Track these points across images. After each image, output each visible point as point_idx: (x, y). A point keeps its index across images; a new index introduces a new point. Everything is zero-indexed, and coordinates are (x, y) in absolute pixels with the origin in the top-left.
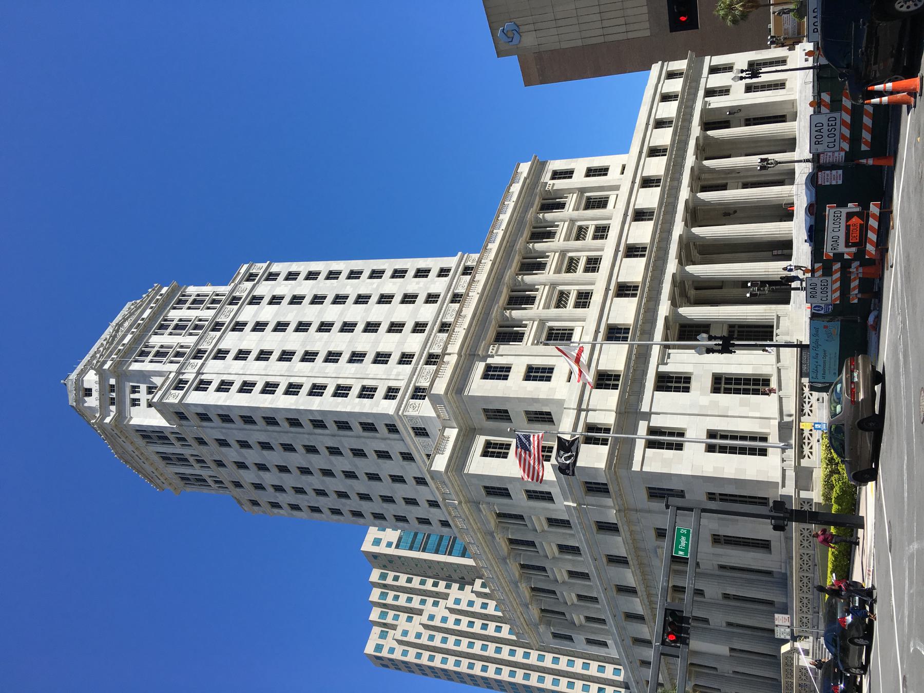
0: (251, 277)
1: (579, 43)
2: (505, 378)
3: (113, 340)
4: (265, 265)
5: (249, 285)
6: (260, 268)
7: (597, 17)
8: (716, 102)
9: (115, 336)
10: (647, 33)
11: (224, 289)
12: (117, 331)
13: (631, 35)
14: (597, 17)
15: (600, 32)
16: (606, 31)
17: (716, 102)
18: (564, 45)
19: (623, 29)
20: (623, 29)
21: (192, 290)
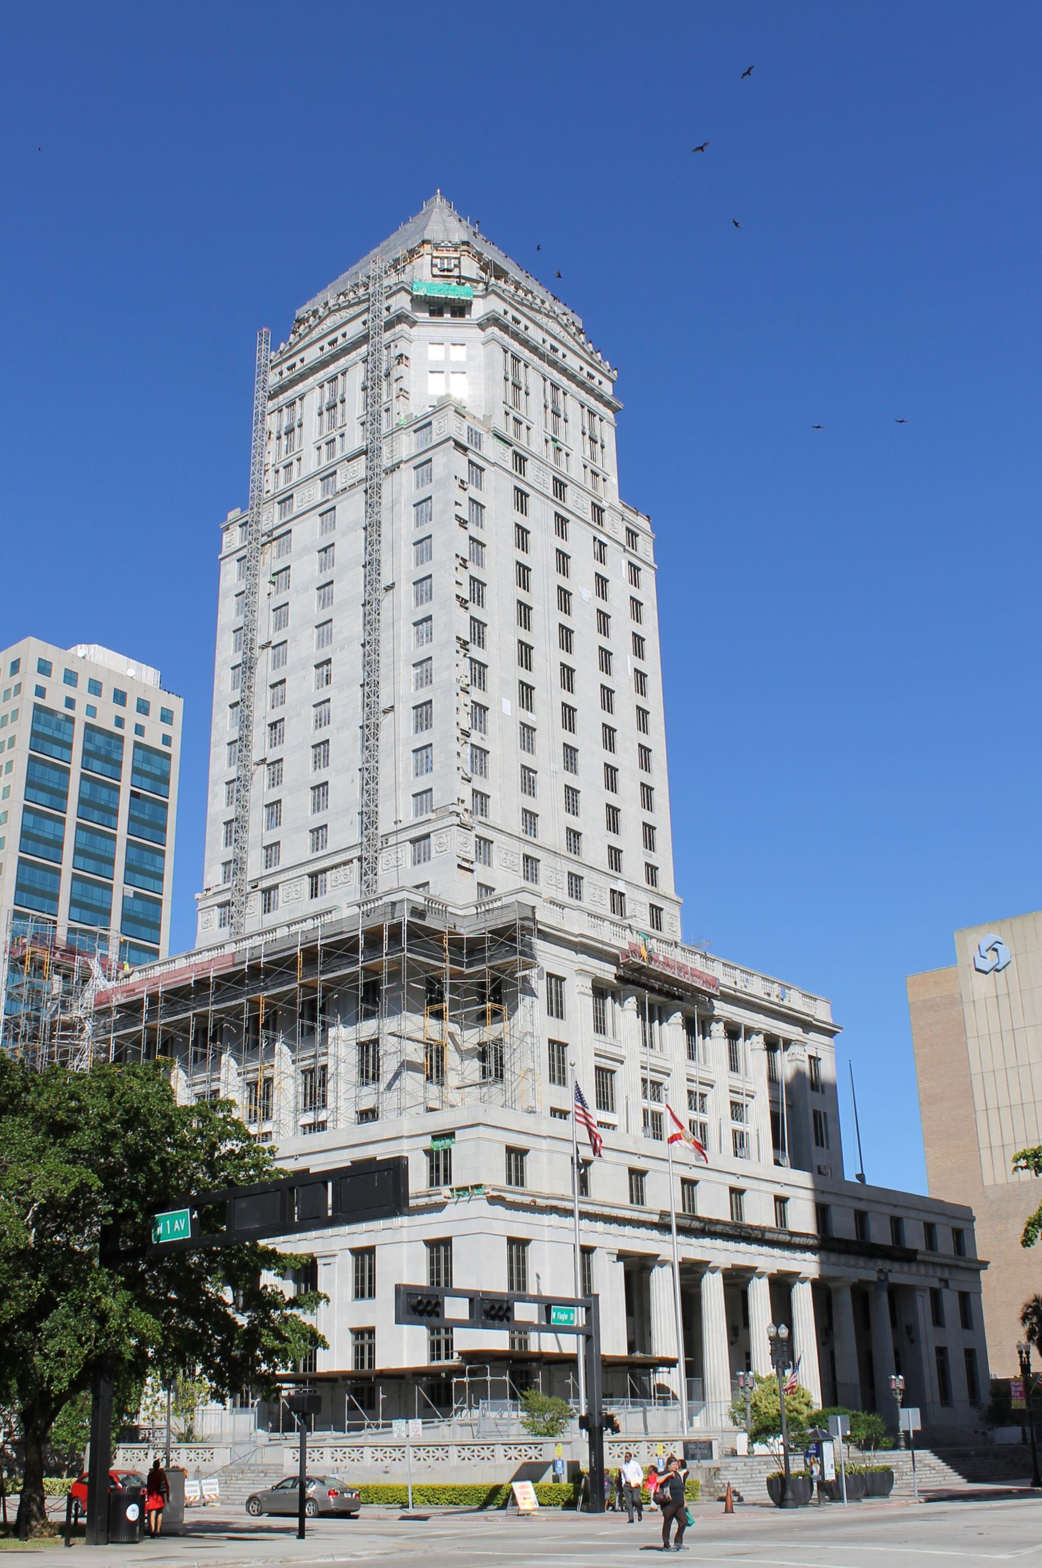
0: (632, 535)
1: (975, 1069)
2: (550, 1013)
3: (532, 309)
4: (651, 559)
5: (622, 537)
6: (645, 546)
7: (1015, 1099)
8: (923, 1305)
9: (539, 311)
10: (988, 1181)
11: (610, 494)
12: (547, 316)
13: (985, 1154)
14: (1015, 1099)
15: (992, 1105)
16: (993, 1114)
17: (923, 1305)
18: (972, 1044)
19: (996, 1142)
20: (996, 1142)
21: (607, 433)
